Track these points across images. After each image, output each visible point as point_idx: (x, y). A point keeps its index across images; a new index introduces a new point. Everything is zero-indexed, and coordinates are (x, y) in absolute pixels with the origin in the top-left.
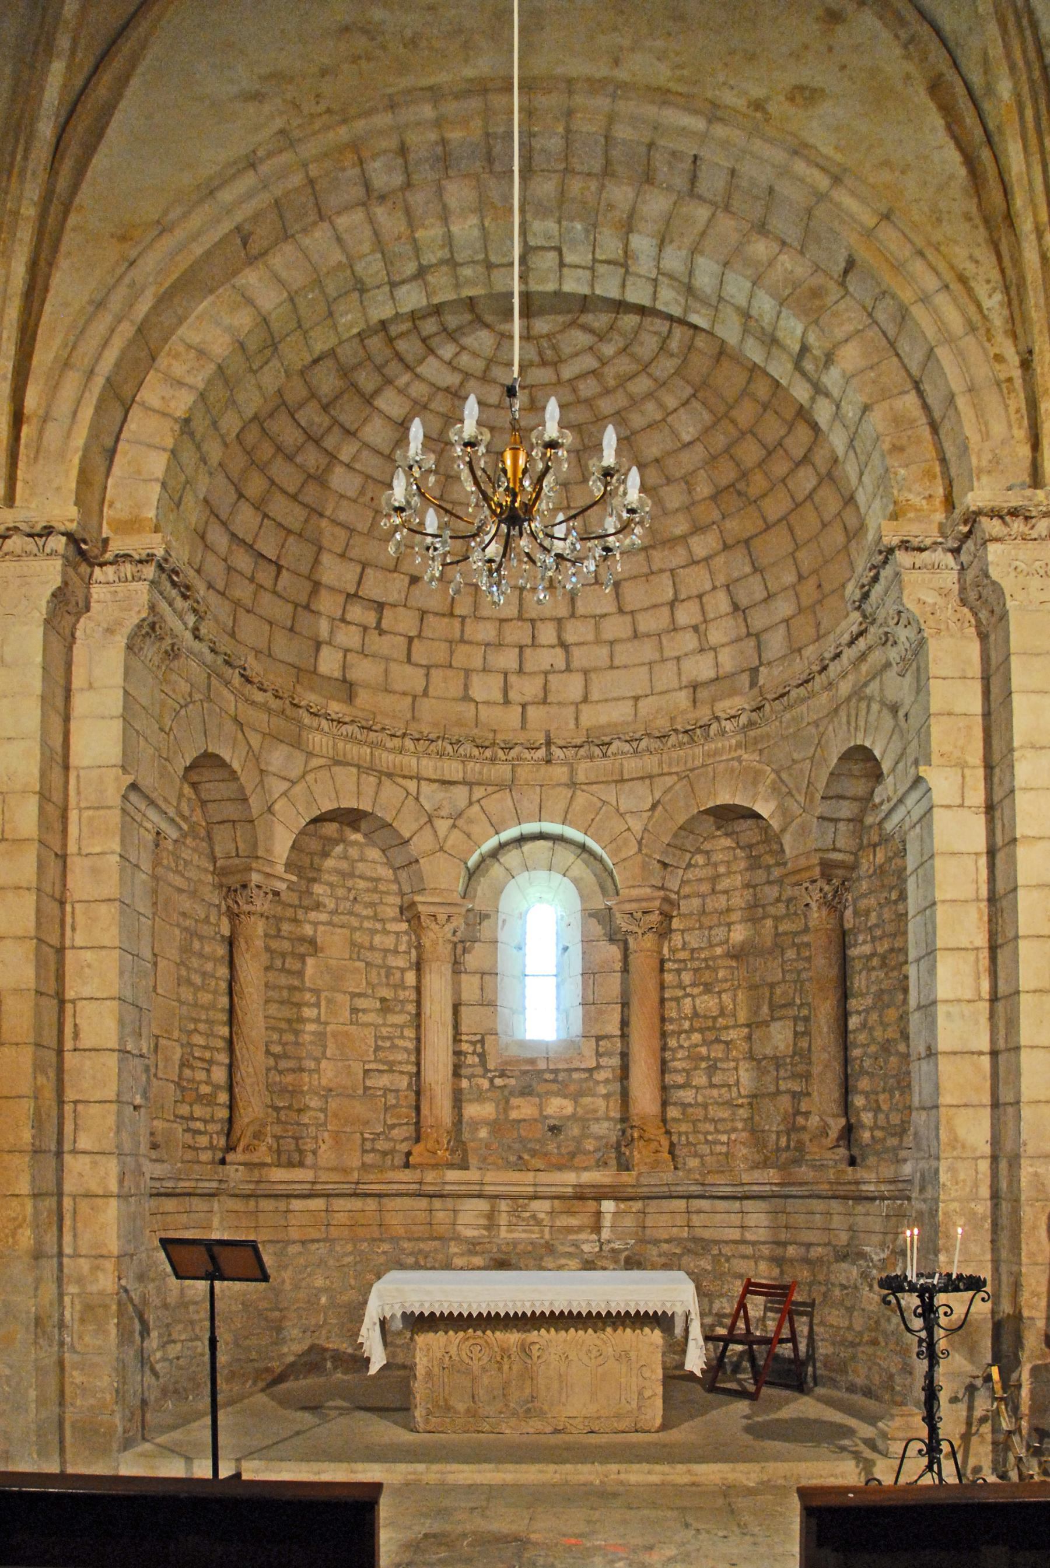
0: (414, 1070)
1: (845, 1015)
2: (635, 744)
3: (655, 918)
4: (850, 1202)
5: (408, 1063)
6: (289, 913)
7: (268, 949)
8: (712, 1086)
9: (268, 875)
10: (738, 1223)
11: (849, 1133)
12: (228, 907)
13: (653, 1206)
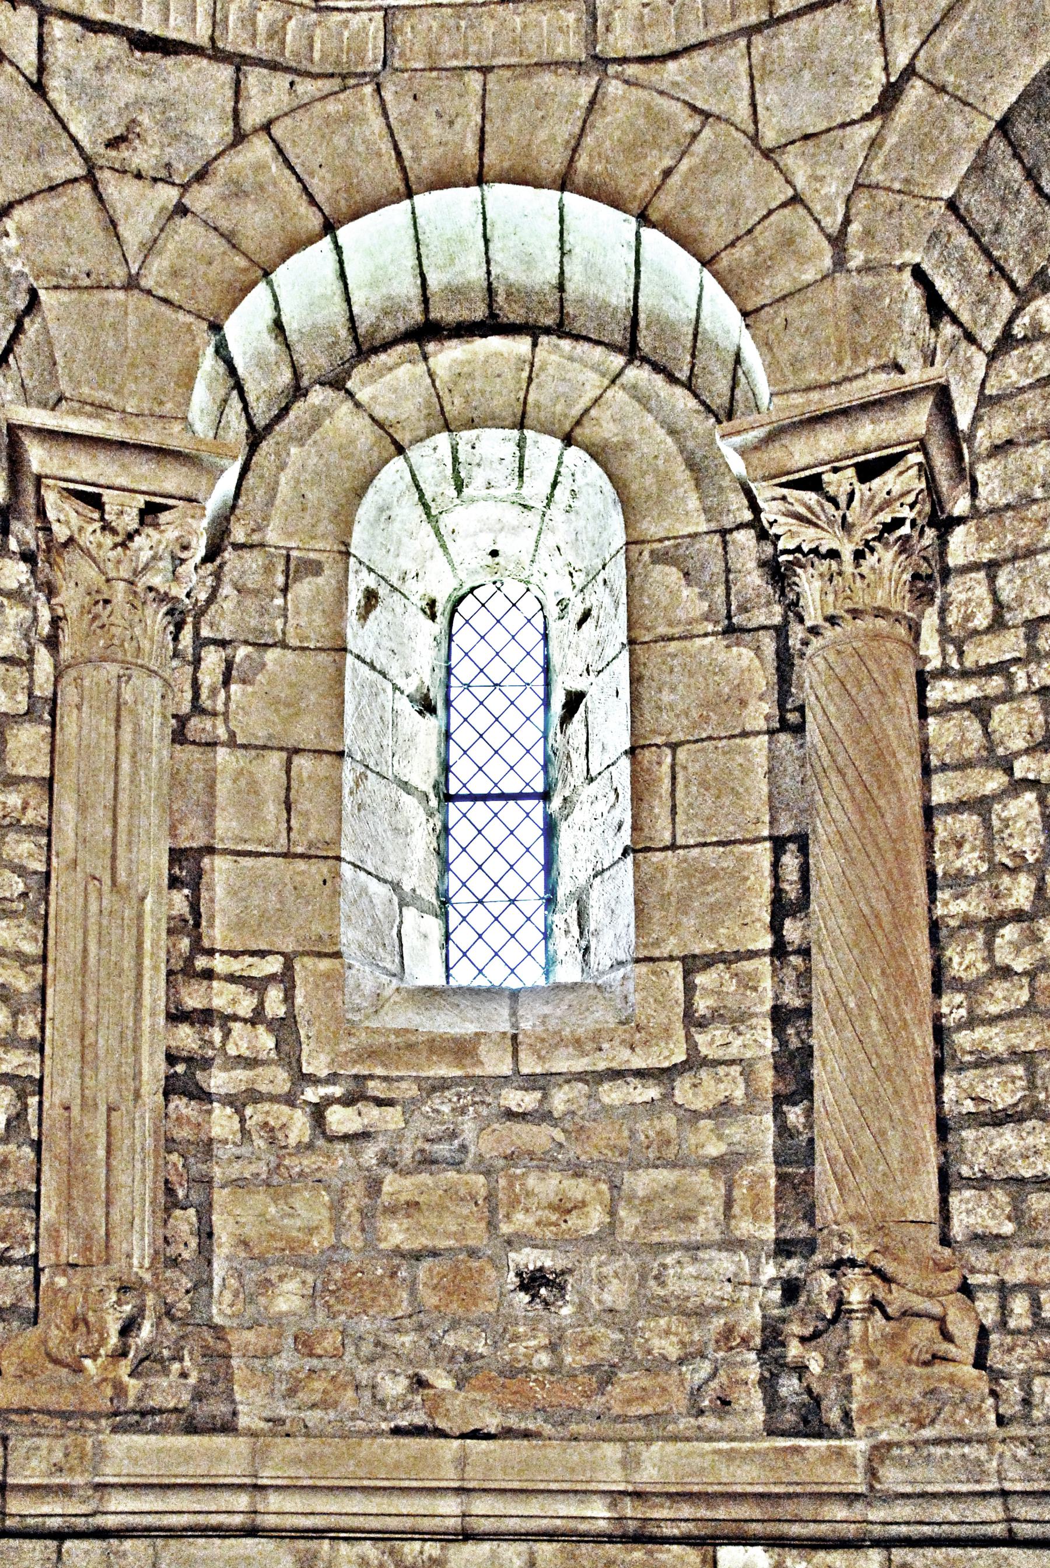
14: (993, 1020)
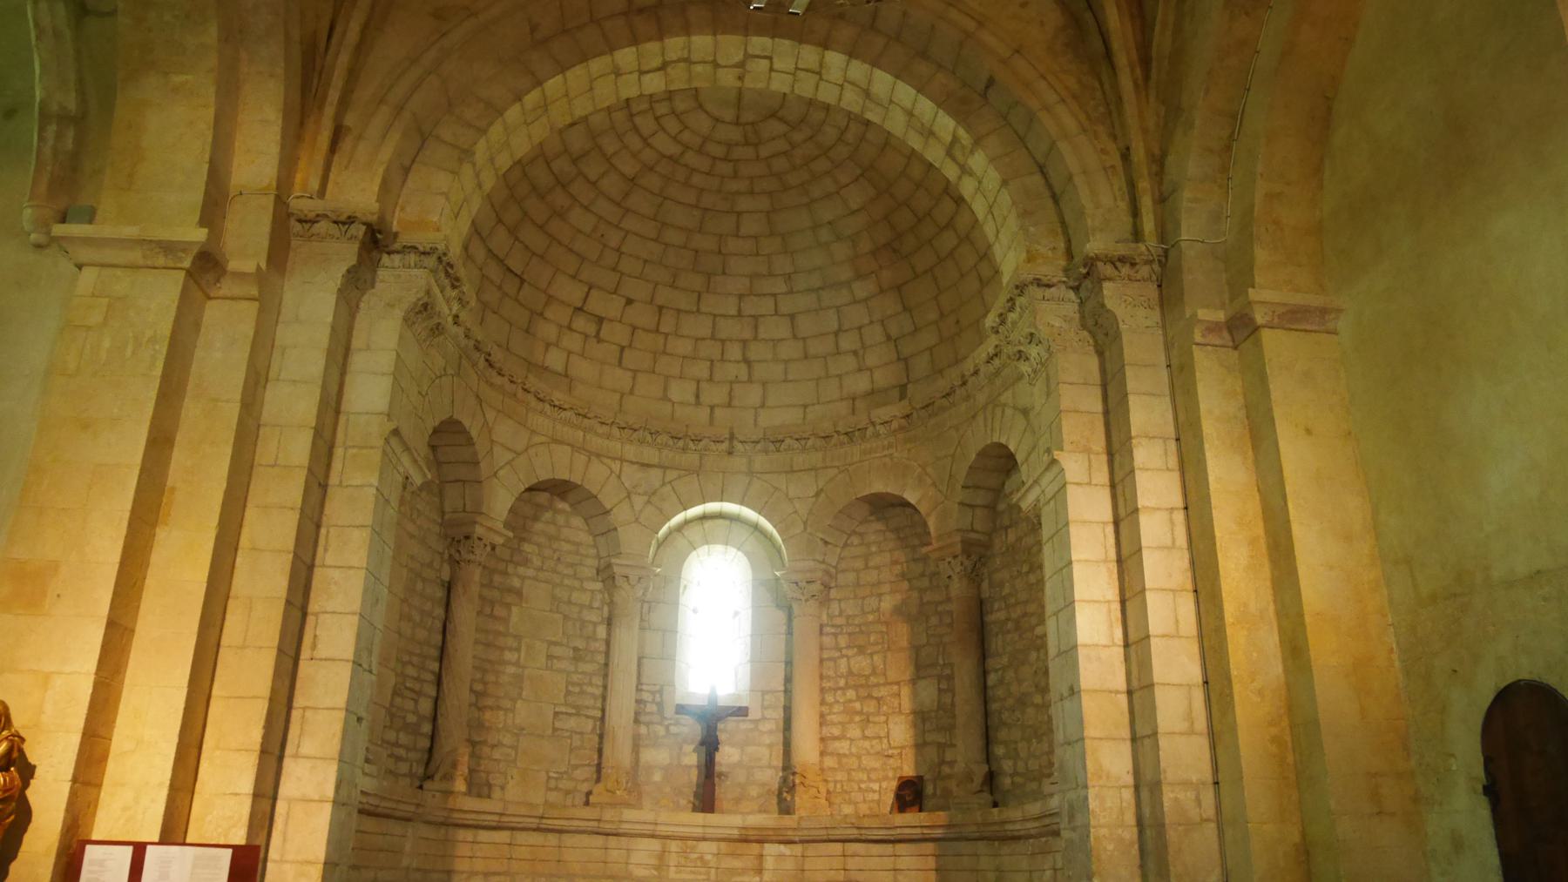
0: (599, 714)
1: (985, 673)
2: (803, 442)
3: (816, 587)
4: (996, 843)
5: (594, 708)
6: (501, 566)
7: (481, 597)
8: (865, 738)
9: (490, 529)
10: (891, 866)
11: (991, 779)
12: (450, 555)
13: (812, 849)
14: (834, 714)
